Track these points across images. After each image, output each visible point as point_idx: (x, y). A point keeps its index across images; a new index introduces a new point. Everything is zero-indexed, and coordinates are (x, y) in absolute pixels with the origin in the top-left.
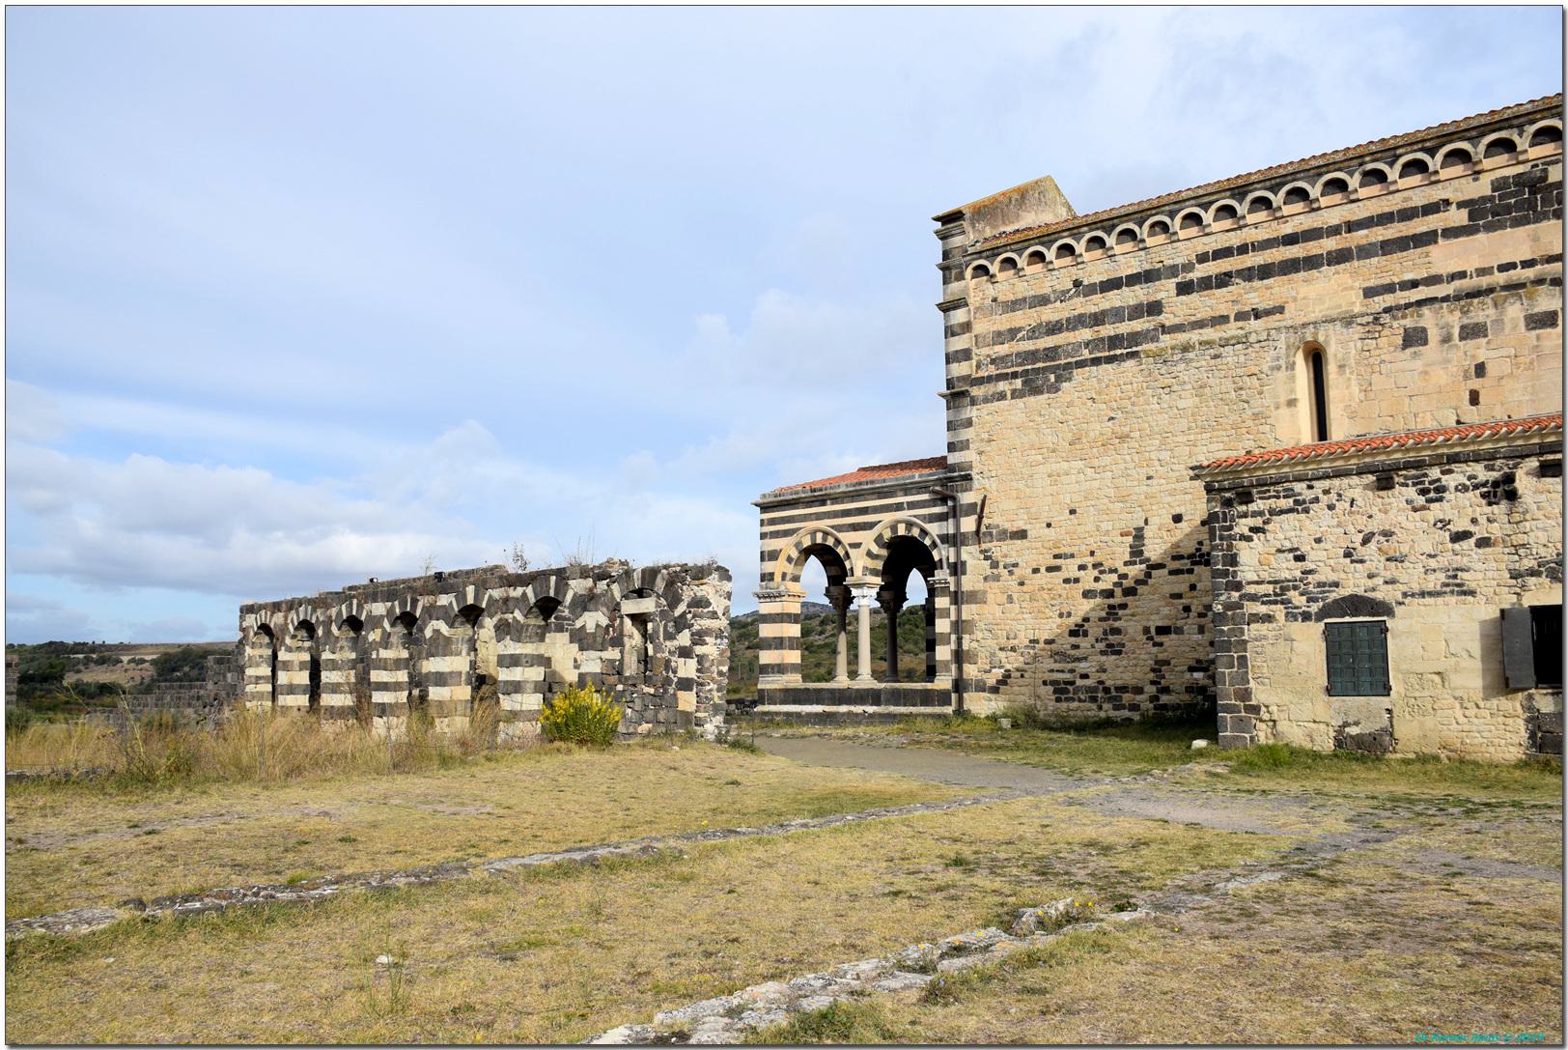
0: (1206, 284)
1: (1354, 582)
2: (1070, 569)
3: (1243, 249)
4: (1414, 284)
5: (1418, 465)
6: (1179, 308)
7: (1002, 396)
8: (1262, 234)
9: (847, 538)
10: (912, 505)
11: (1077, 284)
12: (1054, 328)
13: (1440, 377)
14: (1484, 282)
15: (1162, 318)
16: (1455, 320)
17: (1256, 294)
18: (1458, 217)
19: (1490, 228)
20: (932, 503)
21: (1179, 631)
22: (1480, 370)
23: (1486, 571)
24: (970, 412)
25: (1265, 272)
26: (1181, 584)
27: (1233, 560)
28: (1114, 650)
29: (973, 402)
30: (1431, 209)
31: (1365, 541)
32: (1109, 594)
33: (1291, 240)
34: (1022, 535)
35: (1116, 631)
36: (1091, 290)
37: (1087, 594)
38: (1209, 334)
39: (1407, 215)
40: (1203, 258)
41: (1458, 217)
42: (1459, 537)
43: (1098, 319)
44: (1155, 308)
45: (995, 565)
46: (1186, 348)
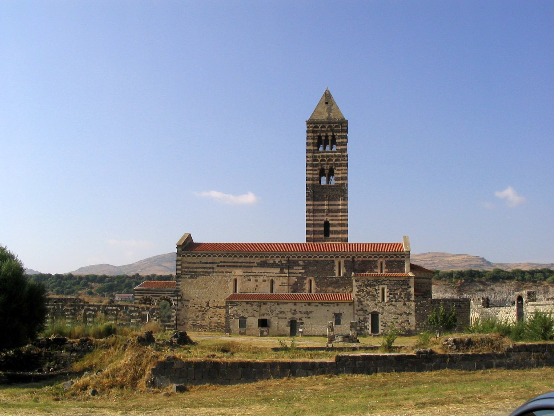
0: (221, 266)
1: (242, 314)
2: (197, 307)
3: (227, 262)
8: (230, 261)
9: (154, 298)
12: (196, 268)
14: (258, 274)
15: (215, 270)
16: (255, 279)
17: (228, 270)
18: (256, 265)
22: (257, 286)
23: (257, 314)
24: (180, 279)
25: (230, 266)
26: (214, 311)
28: (204, 320)
29: (181, 278)
30: (253, 263)
33: (234, 262)
34: (188, 301)
36: (203, 263)
37: (199, 311)
38: (221, 274)
39: (250, 263)
40: (221, 262)
41: (256, 265)
43: (204, 268)
44: (213, 268)
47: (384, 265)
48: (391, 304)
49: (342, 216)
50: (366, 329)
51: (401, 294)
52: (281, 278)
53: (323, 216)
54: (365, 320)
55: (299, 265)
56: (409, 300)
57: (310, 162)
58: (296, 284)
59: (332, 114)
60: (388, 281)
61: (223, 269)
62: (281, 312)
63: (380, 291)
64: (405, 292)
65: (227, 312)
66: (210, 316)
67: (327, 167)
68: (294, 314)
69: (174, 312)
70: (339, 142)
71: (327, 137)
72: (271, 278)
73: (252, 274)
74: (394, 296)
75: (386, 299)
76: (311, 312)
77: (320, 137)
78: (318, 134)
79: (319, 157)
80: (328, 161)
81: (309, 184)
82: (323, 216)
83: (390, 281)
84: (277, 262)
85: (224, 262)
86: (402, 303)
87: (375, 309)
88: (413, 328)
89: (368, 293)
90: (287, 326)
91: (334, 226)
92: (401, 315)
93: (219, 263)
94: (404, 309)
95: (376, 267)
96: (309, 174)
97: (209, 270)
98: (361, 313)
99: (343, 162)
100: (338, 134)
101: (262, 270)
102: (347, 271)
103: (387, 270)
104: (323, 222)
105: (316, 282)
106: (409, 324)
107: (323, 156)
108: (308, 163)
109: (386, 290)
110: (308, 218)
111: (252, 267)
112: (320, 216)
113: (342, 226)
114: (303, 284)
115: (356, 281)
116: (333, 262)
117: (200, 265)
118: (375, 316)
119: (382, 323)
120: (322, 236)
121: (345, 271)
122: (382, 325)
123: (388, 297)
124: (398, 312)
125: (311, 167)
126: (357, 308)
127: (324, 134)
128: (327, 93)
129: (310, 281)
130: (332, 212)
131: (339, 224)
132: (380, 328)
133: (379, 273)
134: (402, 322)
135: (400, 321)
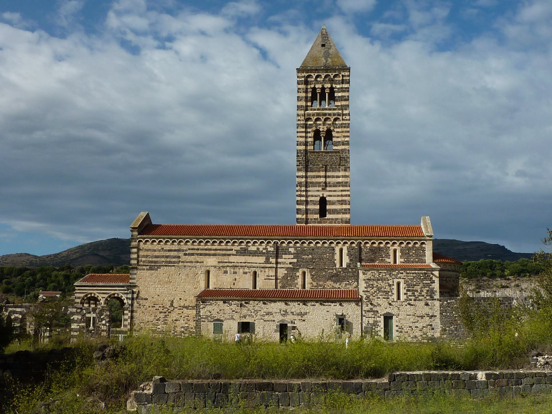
1: (218, 317)
2: (157, 307)
4: (226, 262)
5: (228, 300)
6: (184, 258)
7: (144, 269)
10: (119, 290)
11: (162, 249)
12: (157, 257)
13: (229, 279)
16: (232, 270)
17: (199, 259)
18: (234, 252)
19: (239, 255)
20: (125, 290)
21: (179, 321)
22: (235, 279)
23: (236, 316)
25: (201, 255)
27: (200, 312)
31: (220, 310)
32: (165, 313)
33: (206, 250)
34: (147, 299)
35: (166, 320)
36: (166, 251)
37: (160, 312)
38: (189, 264)
40: (189, 249)
41: (234, 252)
42: (233, 311)
43: (167, 257)
44: (179, 257)
45: (140, 305)
46: (185, 266)
47: (398, 254)
48: (409, 304)
49: (342, 191)
50: (377, 335)
51: (422, 291)
52: (267, 270)
53: (318, 191)
54: (375, 324)
55: (290, 253)
56: (432, 299)
57: (302, 122)
58: (285, 277)
59: (330, 60)
60: (405, 274)
61: (191, 258)
62: (268, 314)
63: (395, 287)
64: (427, 289)
65: (198, 314)
66: (174, 319)
67: (323, 129)
68: (283, 315)
69: (127, 314)
70: (339, 97)
71: (323, 89)
72: (254, 269)
73: (230, 265)
74: (413, 293)
75: (403, 297)
76: (306, 313)
77: (314, 89)
78: (312, 86)
79: (313, 115)
80: (326, 120)
81: (300, 150)
82: (318, 191)
83: (407, 273)
84: (261, 249)
85: (193, 249)
86: (423, 303)
87: (389, 310)
88: (437, 335)
89: (379, 289)
90: (276, 331)
91: (333, 203)
92: (422, 317)
93: (186, 250)
94: (427, 310)
95: (388, 256)
96: (301, 137)
97: (174, 260)
98: (370, 314)
99: (344, 122)
100: (338, 86)
101: (242, 259)
102: (351, 260)
103: (402, 260)
104: (318, 199)
105: (311, 275)
106: (433, 329)
107: (318, 114)
108: (299, 122)
109: (402, 286)
110: (299, 193)
111: (229, 255)
112: (313, 191)
113: (342, 204)
114: (295, 278)
115: (364, 274)
116: (333, 249)
117: (162, 253)
118: (388, 318)
119: (397, 328)
120: (317, 216)
121: (348, 261)
122: (397, 331)
123: (405, 294)
124: (418, 313)
125: (303, 128)
126: (365, 308)
127: (320, 86)
128: (324, 33)
129: (304, 273)
130: (330, 186)
131: (338, 201)
132: (395, 334)
133: (392, 263)
134: (424, 327)
135: (420, 325)
